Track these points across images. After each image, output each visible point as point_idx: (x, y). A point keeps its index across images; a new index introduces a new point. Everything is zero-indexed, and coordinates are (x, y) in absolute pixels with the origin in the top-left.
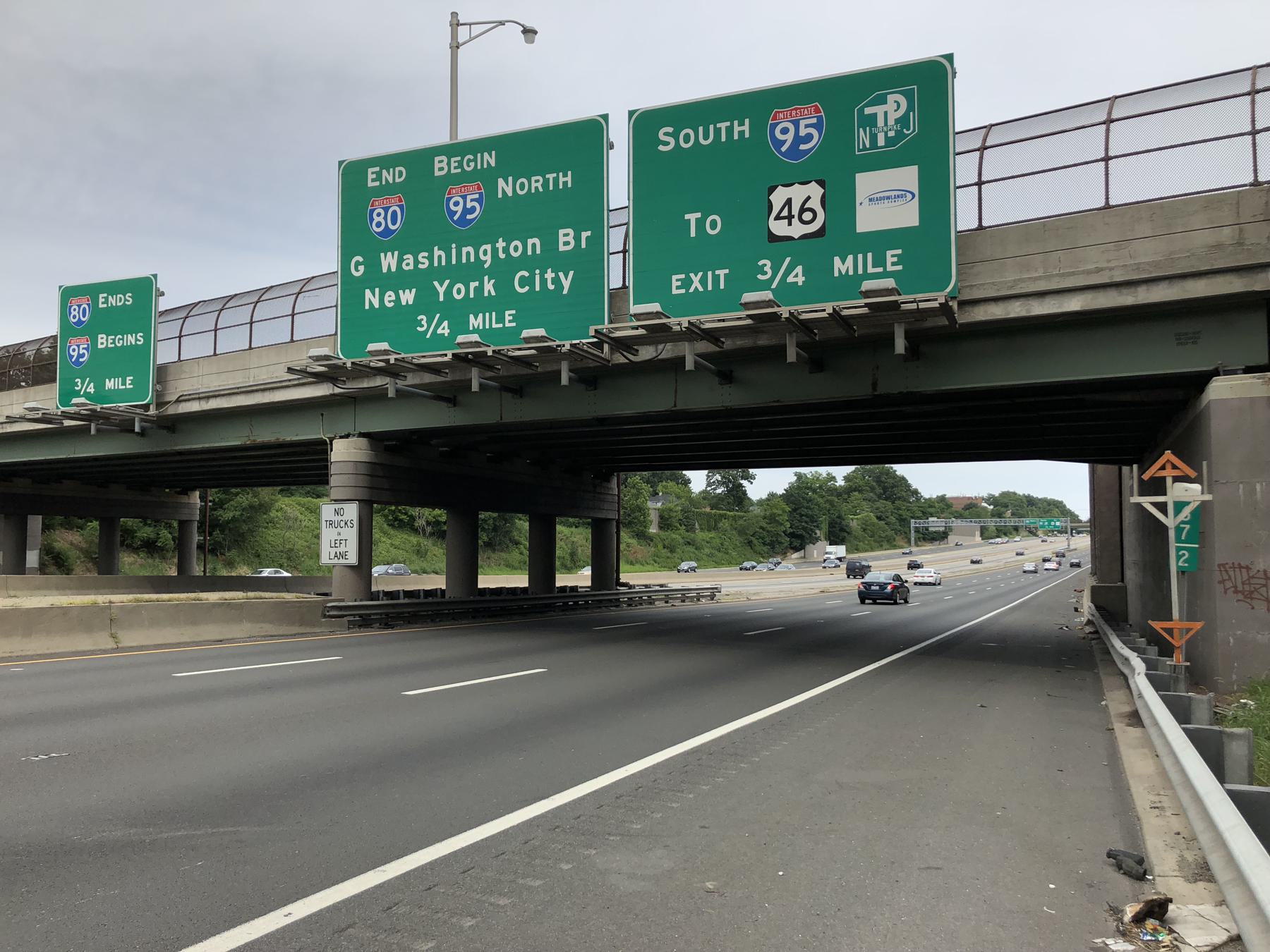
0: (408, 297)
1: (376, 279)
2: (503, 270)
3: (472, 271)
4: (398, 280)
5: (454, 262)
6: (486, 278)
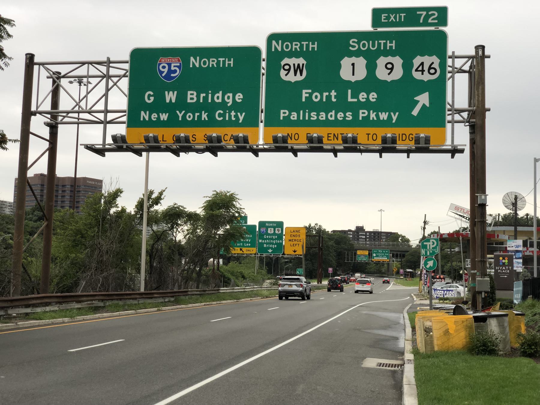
6: (203, 112)
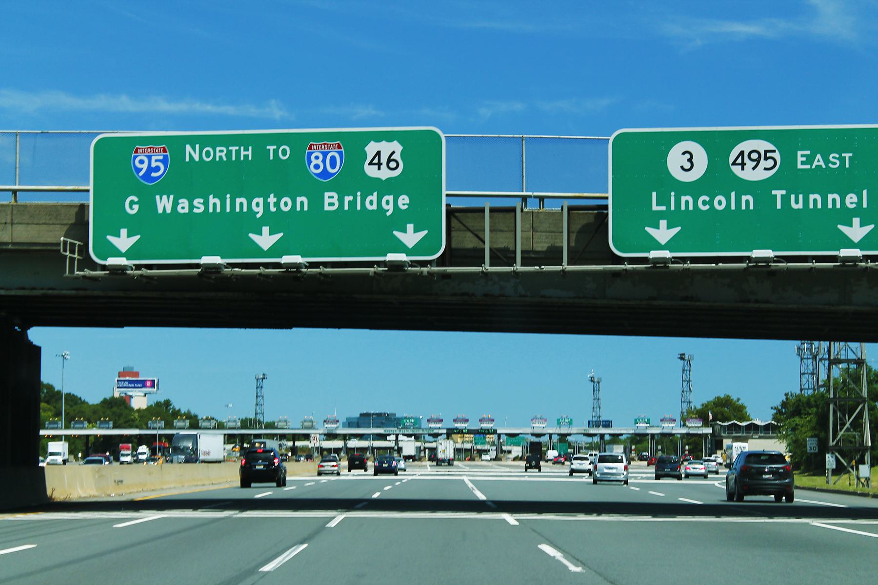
5: (228, 210)
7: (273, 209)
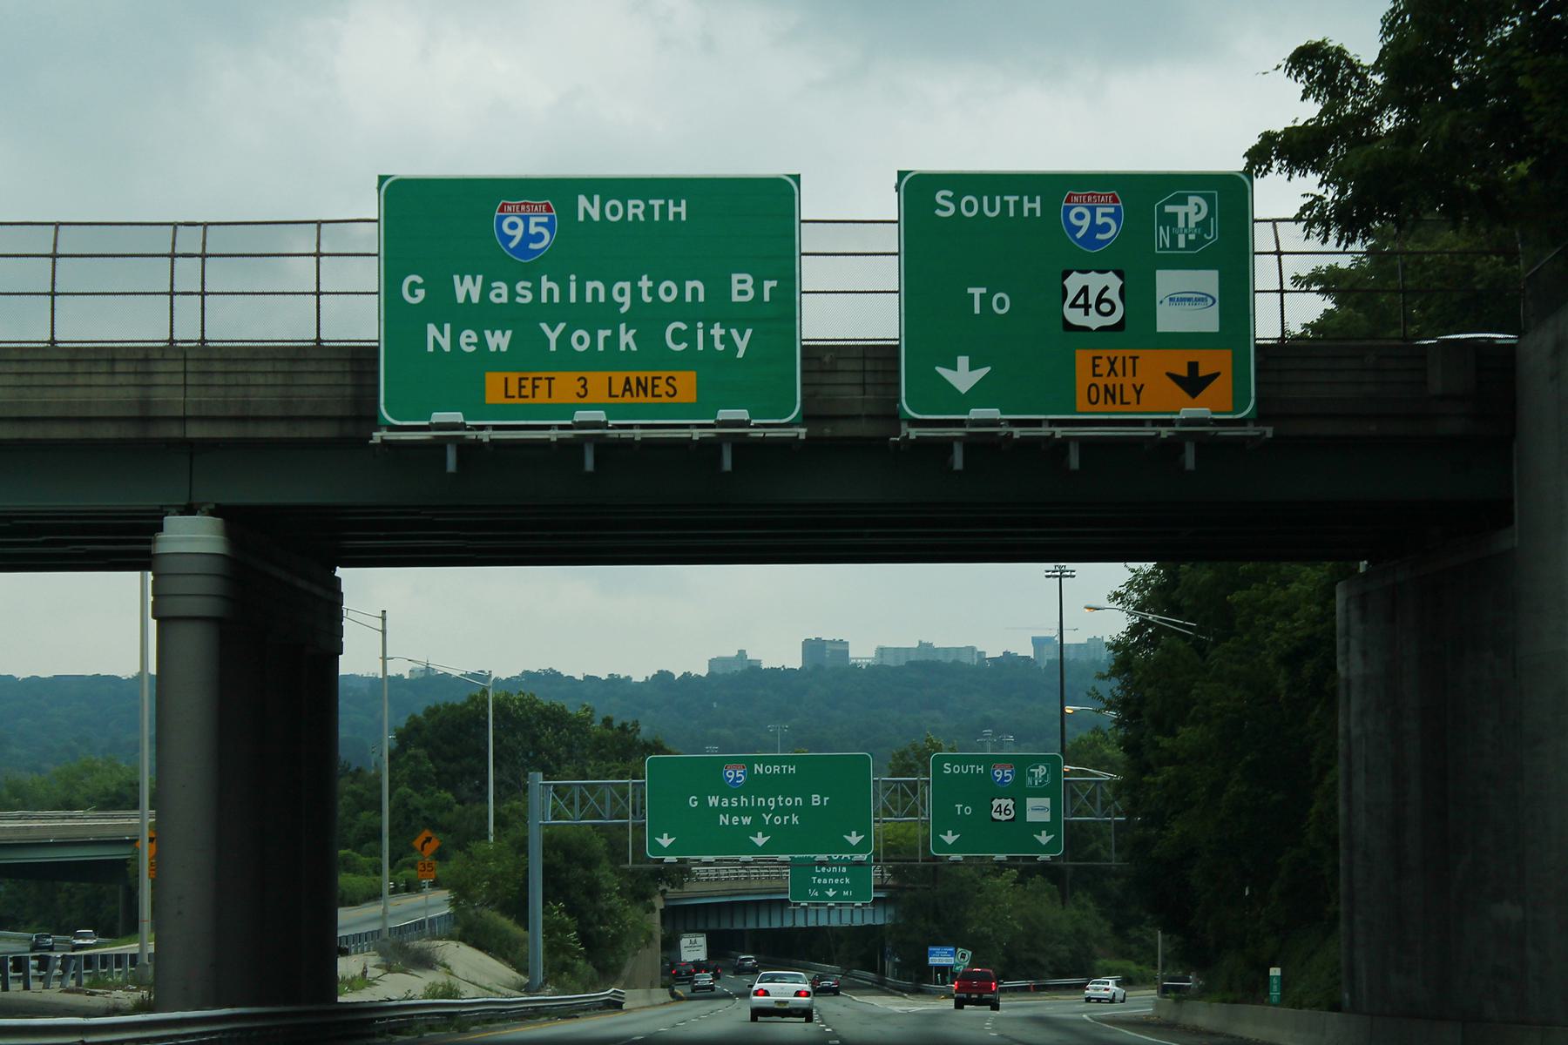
0: (499, 341)
1: (442, 307)
2: (648, 318)
3: (606, 314)
4: (482, 315)
7: (647, 299)
